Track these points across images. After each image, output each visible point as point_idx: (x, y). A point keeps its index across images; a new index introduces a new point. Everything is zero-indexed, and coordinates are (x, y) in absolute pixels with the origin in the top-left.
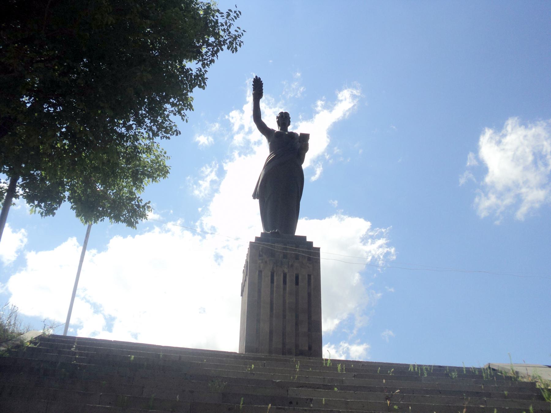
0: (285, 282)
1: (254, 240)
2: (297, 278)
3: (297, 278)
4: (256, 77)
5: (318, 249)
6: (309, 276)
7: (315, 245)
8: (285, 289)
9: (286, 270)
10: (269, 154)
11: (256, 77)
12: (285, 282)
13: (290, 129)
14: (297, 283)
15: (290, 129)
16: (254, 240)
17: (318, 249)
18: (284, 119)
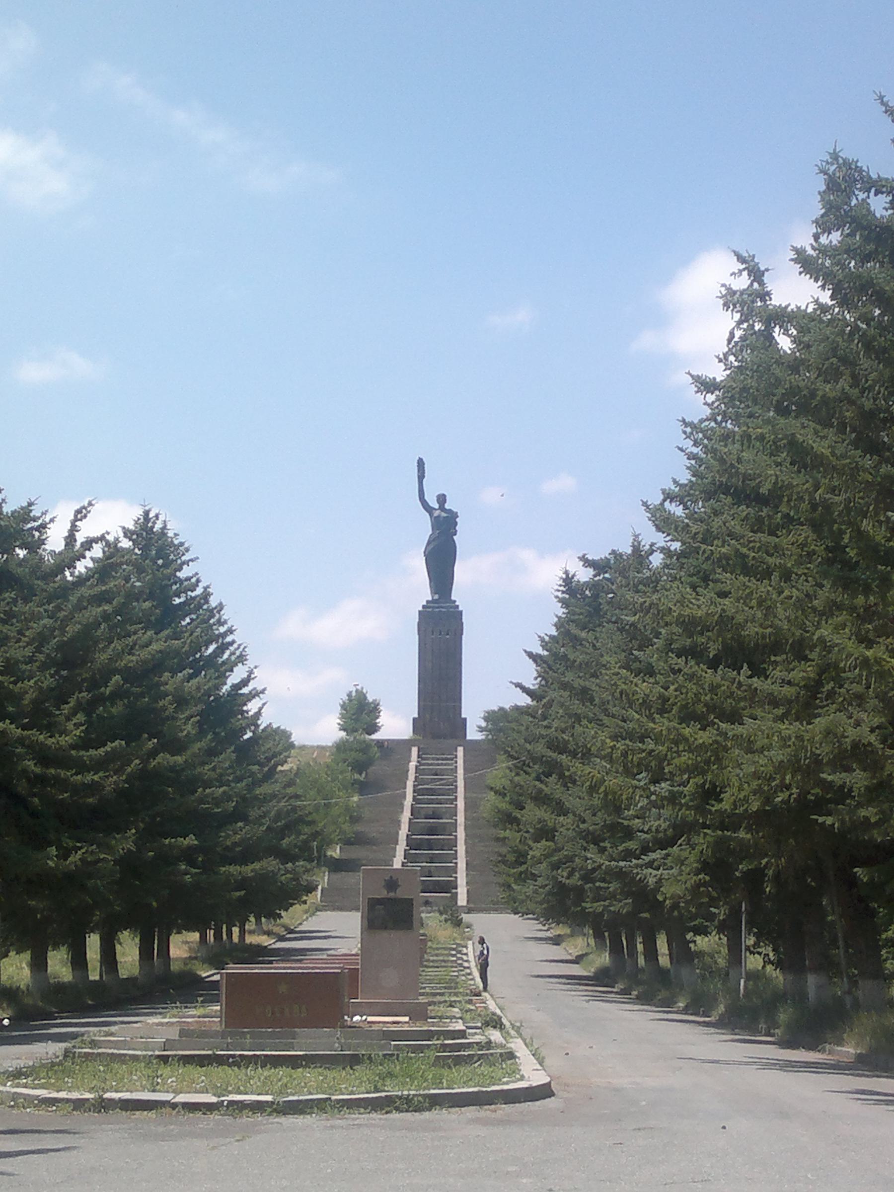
1: (421, 609)
13: (447, 506)
15: (447, 506)
16: (421, 609)
18: (442, 499)
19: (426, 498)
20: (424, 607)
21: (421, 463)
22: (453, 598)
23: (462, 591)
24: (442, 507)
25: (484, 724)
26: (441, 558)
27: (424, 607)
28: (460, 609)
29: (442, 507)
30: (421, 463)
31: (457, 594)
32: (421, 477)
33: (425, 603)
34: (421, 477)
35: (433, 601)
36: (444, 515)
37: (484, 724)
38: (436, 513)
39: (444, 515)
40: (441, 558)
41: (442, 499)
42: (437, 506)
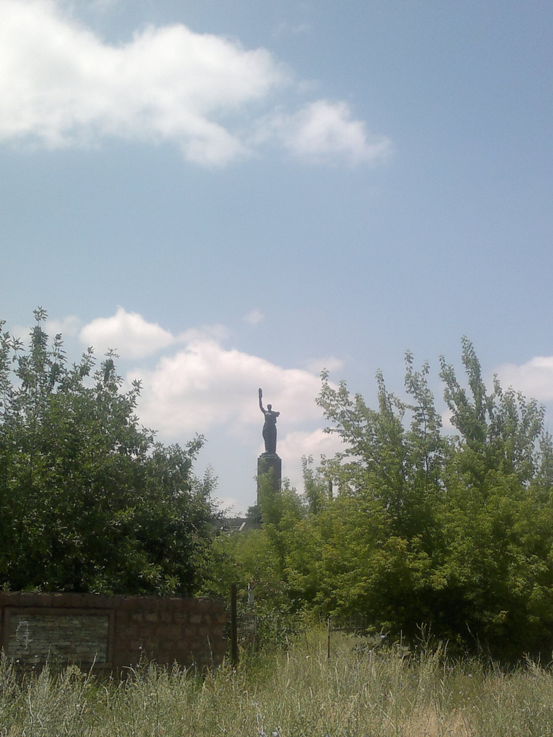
13: (272, 410)
15: (272, 410)
18: (269, 407)
19: (263, 406)
21: (260, 391)
23: (281, 451)
24: (270, 411)
29: (270, 411)
30: (260, 391)
32: (261, 396)
34: (261, 396)
36: (270, 414)
38: (267, 414)
39: (270, 414)
40: (270, 434)
41: (269, 407)
42: (267, 410)
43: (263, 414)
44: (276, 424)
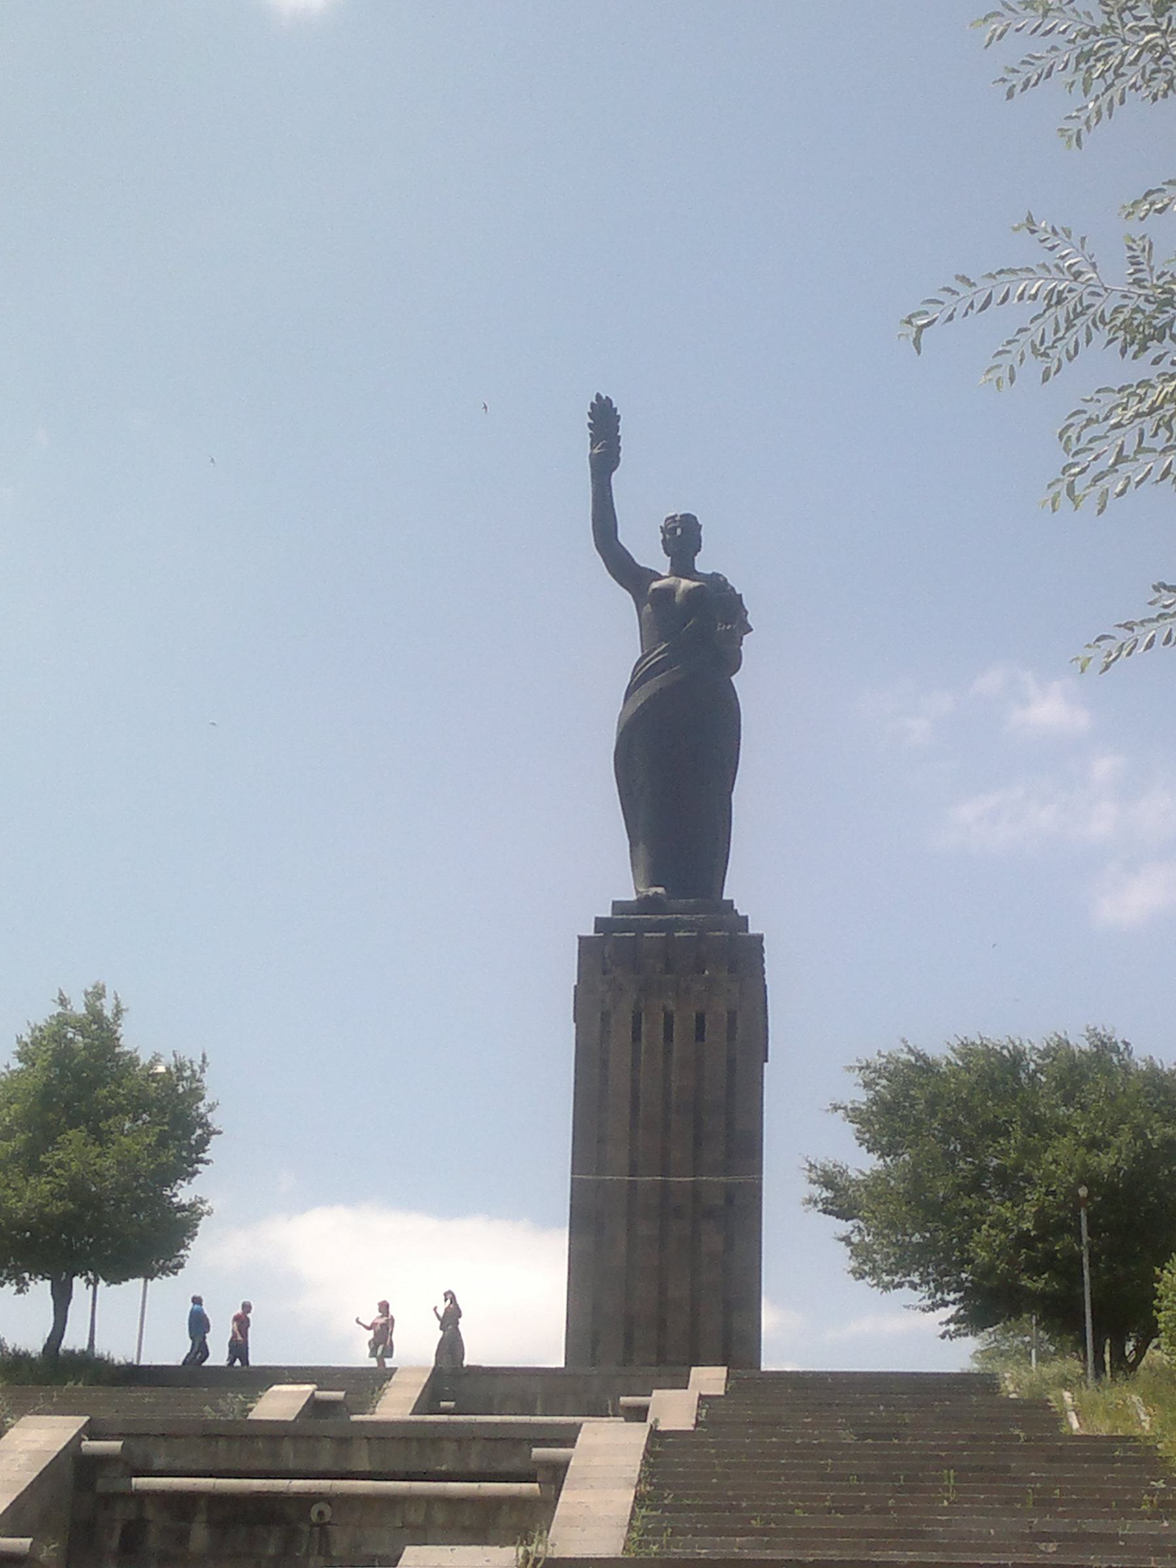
0: (668, 1037)
1: (590, 932)
2: (700, 1019)
3: (700, 1019)
4: (598, 396)
5: (760, 938)
6: (732, 1015)
7: (752, 930)
8: (668, 1053)
9: (671, 1006)
10: (640, 655)
11: (598, 396)
12: (668, 1037)
13: (703, 564)
14: (700, 1036)
16: (590, 932)
17: (760, 938)
18: (683, 537)
20: (600, 923)
21: (604, 420)
22: (725, 897)
24: (683, 563)
25: (862, 1163)
26: (679, 756)
27: (600, 923)
28: (752, 930)
29: (683, 563)
30: (604, 420)
31: (745, 885)
33: (608, 914)
35: (645, 904)
37: (862, 1163)
39: (685, 584)
40: (679, 756)
41: (683, 537)
43: (625, 599)
44: (733, 678)
